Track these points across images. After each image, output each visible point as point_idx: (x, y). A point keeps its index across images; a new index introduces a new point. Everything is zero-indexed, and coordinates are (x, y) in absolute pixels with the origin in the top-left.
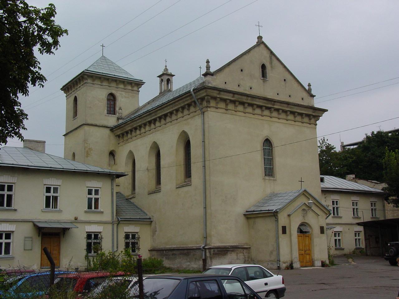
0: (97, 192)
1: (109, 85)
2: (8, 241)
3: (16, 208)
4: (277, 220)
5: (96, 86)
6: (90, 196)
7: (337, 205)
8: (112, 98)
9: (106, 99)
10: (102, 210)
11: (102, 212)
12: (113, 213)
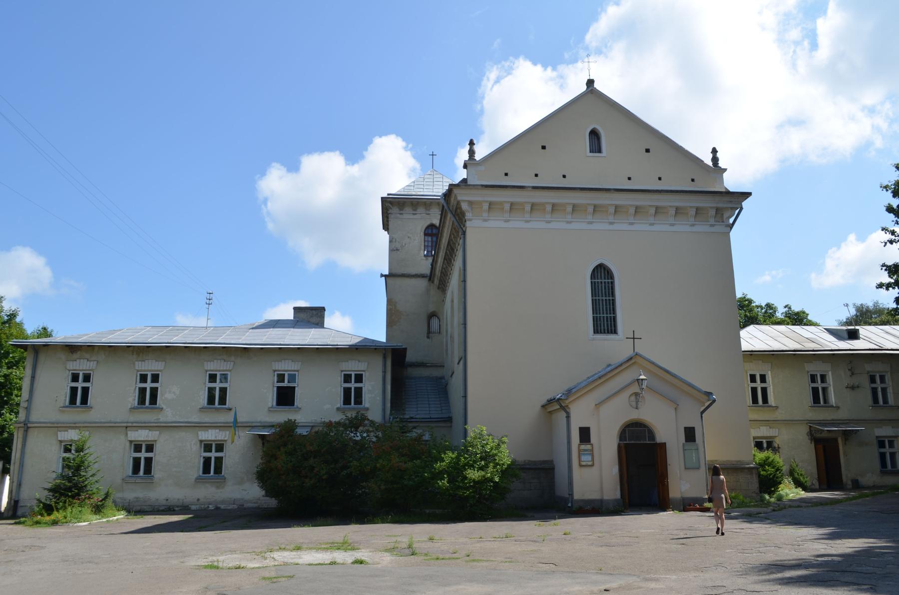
0: (359, 378)
2: (219, 454)
4: (568, 417)
5: (405, 216)
6: (347, 385)
9: (422, 234)
10: (367, 405)
12: (384, 410)
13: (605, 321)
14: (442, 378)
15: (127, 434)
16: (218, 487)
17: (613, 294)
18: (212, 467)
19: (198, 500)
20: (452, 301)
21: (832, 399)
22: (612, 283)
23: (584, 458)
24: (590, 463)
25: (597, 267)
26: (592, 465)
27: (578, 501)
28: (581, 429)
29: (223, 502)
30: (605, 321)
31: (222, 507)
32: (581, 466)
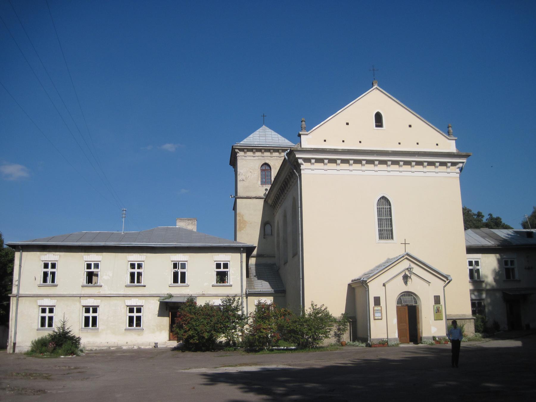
0: (226, 266)
1: (262, 155)
3: (145, 284)
5: (248, 158)
7: (511, 265)
8: (267, 168)
10: (231, 283)
11: (231, 286)
12: (242, 286)
13: (386, 231)
14: (275, 264)
15: (80, 302)
16: (139, 335)
17: (391, 215)
18: (135, 322)
19: (127, 343)
20: (285, 216)
21: (517, 276)
22: (390, 208)
23: (376, 315)
24: (380, 318)
25: (380, 198)
26: (381, 319)
27: (374, 339)
28: (375, 297)
29: (142, 344)
30: (386, 231)
31: (143, 347)
32: (375, 319)
